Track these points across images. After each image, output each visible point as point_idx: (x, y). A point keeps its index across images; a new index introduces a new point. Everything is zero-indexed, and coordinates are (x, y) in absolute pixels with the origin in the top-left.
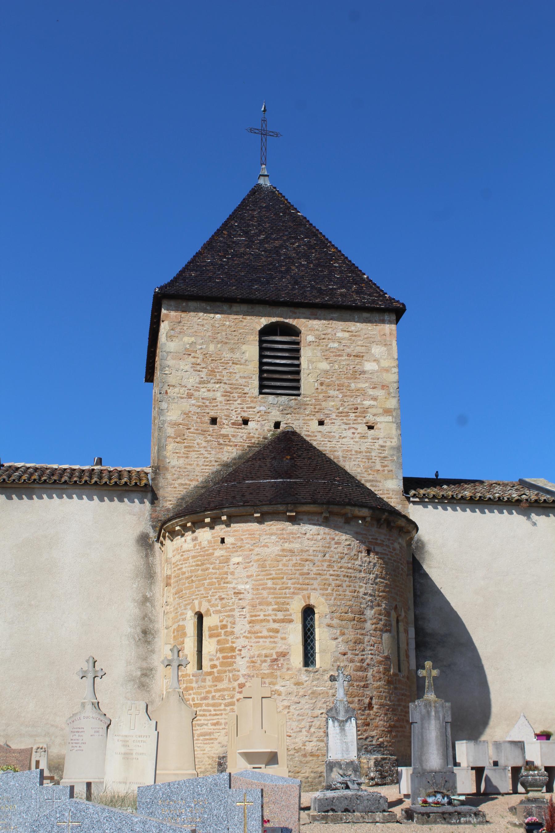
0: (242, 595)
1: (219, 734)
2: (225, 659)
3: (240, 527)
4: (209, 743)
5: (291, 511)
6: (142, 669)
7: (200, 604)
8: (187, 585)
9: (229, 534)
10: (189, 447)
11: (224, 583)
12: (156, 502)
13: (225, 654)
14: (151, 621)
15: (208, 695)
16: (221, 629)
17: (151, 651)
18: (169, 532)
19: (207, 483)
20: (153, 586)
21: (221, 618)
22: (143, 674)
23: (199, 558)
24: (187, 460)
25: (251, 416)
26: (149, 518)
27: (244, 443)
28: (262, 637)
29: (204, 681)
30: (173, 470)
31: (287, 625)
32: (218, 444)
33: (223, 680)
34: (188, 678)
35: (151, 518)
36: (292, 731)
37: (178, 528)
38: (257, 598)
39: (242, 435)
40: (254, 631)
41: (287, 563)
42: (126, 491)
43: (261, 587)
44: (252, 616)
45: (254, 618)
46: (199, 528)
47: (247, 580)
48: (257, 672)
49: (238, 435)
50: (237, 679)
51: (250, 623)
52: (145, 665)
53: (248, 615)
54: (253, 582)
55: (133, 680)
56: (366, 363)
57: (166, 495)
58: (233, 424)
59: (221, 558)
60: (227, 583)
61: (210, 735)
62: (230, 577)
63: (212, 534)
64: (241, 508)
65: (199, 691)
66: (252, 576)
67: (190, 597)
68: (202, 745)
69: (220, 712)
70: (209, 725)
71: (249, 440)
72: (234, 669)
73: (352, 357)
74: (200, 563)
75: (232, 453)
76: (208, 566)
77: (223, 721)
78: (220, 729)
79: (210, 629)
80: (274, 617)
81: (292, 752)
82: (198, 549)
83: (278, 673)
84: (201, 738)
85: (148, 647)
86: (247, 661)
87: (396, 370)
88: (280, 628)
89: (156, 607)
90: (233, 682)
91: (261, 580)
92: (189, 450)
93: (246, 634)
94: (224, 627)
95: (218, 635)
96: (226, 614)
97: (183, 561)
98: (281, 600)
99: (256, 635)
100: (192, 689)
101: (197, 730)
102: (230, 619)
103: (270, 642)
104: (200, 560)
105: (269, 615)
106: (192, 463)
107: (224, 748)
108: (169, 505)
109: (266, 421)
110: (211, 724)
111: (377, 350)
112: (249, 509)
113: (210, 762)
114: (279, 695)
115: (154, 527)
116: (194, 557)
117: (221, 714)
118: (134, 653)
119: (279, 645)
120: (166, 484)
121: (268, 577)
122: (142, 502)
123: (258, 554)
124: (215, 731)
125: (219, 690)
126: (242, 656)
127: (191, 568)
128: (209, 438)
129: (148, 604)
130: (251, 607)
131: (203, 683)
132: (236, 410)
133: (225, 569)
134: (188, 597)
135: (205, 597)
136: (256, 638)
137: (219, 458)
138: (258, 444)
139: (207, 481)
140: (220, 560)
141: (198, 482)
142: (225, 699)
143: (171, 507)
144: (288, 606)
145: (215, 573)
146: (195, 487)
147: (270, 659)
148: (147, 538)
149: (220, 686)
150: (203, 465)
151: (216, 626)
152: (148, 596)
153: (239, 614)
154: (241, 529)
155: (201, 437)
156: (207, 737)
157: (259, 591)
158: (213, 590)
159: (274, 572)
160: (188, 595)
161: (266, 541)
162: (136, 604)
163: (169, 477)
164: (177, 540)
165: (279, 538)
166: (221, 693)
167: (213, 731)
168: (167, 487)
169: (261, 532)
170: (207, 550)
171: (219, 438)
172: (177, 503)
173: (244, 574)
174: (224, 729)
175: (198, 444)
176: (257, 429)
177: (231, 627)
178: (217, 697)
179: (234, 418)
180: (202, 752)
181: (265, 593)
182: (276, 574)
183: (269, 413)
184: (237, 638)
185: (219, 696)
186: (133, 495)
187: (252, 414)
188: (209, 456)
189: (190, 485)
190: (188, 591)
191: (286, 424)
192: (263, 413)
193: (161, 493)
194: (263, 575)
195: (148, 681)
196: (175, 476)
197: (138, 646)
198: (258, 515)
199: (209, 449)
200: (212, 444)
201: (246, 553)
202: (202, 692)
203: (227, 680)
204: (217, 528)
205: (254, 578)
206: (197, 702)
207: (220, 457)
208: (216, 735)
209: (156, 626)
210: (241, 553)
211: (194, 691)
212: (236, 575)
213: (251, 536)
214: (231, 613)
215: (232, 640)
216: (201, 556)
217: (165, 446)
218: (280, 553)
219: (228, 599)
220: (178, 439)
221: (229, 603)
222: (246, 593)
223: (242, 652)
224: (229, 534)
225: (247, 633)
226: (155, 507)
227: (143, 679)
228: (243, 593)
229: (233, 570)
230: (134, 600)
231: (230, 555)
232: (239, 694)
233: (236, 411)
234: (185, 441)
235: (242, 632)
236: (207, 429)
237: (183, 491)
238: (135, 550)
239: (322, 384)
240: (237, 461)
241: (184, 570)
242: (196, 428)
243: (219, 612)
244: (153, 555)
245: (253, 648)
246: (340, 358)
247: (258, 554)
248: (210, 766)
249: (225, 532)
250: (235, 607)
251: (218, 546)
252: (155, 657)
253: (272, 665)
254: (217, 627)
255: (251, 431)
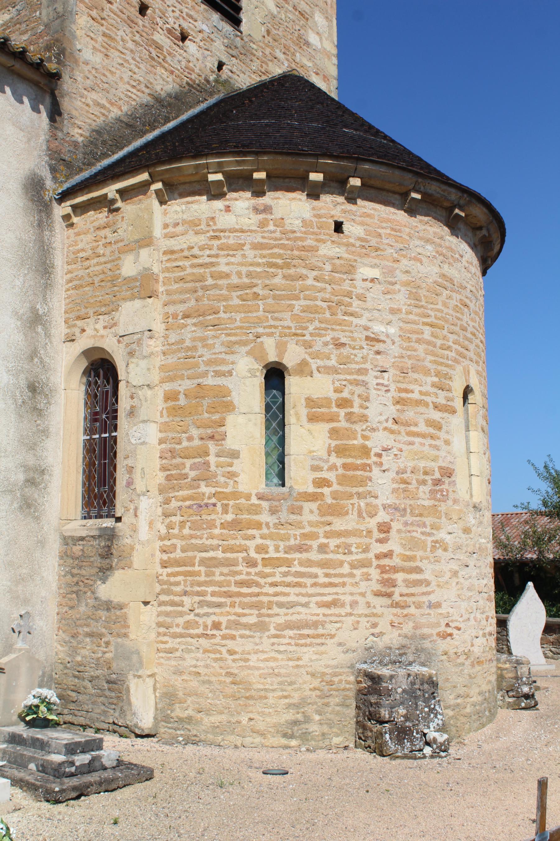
0: (381, 344)
1: (338, 625)
2: (349, 470)
3: (373, 209)
4: (311, 645)
5: (461, 209)
6: (27, 468)
7: (281, 348)
8: (236, 302)
9: (353, 217)
10: (110, 37)
11: (345, 314)
12: (58, 118)
13: (350, 460)
14: (44, 367)
15: (309, 543)
16: (338, 406)
17: (43, 431)
18: (164, 184)
19: (133, 119)
20: (48, 292)
21: (337, 384)
22: (27, 481)
23: (276, 250)
24: (106, 60)
25: (191, 33)
26: (44, 147)
27: (182, 73)
28: (418, 435)
29: (298, 511)
30: (86, 68)
31: (449, 416)
32: (150, 57)
33: (347, 513)
34: (243, 501)
35: (49, 149)
36: (461, 619)
37: (212, 177)
38: (409, 357)
39: (181, 58)
40: (404, 421)
41: (447, 301)
42: (11, 71)
43: (414, 337)
44: (400, 390)
45: (404, 395)
46: (276, 189)
47: (390, 317)
48: (412, 502)
49: (175, 56)
50: (373, 513)
51: (398, 402)
52: (31, 461)
53: (393, 387)
54: (401, 324)
55: (11, 491)
56: (310, 31)
57: (74, 113)
58: (169, 31)
59: (337, 262)
60: (352, 315)
61: (316, 628)
62: (356, 303)
63: (313, 209)
64: (397, 172)
65: (282, 532)
66: (399, 310)
67: (248, 328)
68: (290, 648)
69: (341, 580)
70: (311, 605)
71: (188, 73)
72: (370, 492)
73: (297, 13)
74: (279, 261)
75: (167, 82)
76: (304, 271)
77: (348, 599)
78: (340, 615)
79: (310, 402)
80: (435, 400)
81: (461, 659)
82: (274, 232)
83: (443, 507)
84: (291, 633)
85: (38, 422)
86: (393, 480)
87: (335, 61)
88: (443, 422)
89: (53, 340)
90: (368, 519)
91: (414, 322)
92: (109, 42)
93: (390, 424)
94: (344, 403)
95: (332, 419)
96: (348, 377)
97: (220, 248)
98: (443, 368)
99: (408, 429)
100: (258, 525)
101: (278, 615)
102: (359, 390)
103: (430, 445)
104: (280, 256)
105: (427, 394)
106: (113, 70)
107: (350, 655)
108: (77, 136)
109: (209, 53)
110: (317, 603)
111: (319, 19)
112: (408, 179)
113: (316, 683)
114: (445, 550)
115: (53, 170)
116: (256, 246)
117: (344, 584)
118: (12, 430)
119: (442, 454)
120: (74, 91)
121: (425, 320)
122: (36, 109)
123: (407, 272)
124: (327, 619)
125: (339, 534)
126: (383, 468)
127: (251, 269)
128: (137, 38)
129: (40, 329)
130: (398, 373)
131: (293, 517)
132: (174, 9)
133: (346, 286)
134: (241, 328)
135: (295, 334)
136: (409, 434)
137: (151, 83)
138: (199, 85)
139: (133, 116)
140: (334, 265)
141: (122, 111)
142: (350, 553)
143: (80, 139)
144: (451, 383)
145: (323, 290)
146: (116, 119)
147: (432, 479)
148: (41, 188)
149: (339, 524)
150: (128, 83)
151: (326, 398)
152: (40, 312)
153: (376, 381)
154: (376, 213)
155: (128, 30)
156: (306, 632)
157: (412, 344)
158: (317, 324)
159: (432, 313)
160: (238, 324)
161: (419, 250)
162: (19, 323)
163: (79, 79)
164: (188, 203)
165: (437, 252)
166: (343, 539)
167: (324, 619)
168: (75, 98)
169: (412, 232)
170: (302, 239)
171: (151, 46)
172: (91, 137)
173: (385, 304)
174: (351, 614)
175: (123, 40)
176: (198, 60)
177: (361, 406)
178: (332, 548)
179: (171, 20)
180: (291, 663)
181: (421, 349)
182: (435, 316)
183: (212, 40)
184: (373, 430)
185: (338, 547)
186: (22, 86)
187: (193, 30)
188: (136, 70)
189: (109, 111)
190: (239, 316)
191: (232, 72)
192: (206, 35)
193: (66, 104)
194: (416, 315)
195: (36, 496)
196: (88, 82)
197: (21, 416)
198: (418, 196)
199: (138, 59)
200: (141, 50)
201: (387, 263)
202: (289, 535)
203: (355, 513)
204: (327, 199)
205: (403, 316)
206: (272, 554)
207: (151, 80)
208: (331, 628)
209: (52, 378)
210: (376, 261)
211: (265, 531)
212: (369, 304)
213: (395, 233)
214: (360, 378)
215: (364, 433)
216: (283, 247)
217: (74, 13)
218: (440, 280)
219: (354, 348)
220: (94, 13)
221: (356, 355)
222: (388, 341)
223: (384, 459)
224: (353, 217)
225: (391, 421)
226: (56, 128)
227: (28, 491)
228: (384, 342)
229: (360, 291)
230: (17, 313)
231: (355, 261)
232: (378, 544)
233: (173, 11)
234: (103, 22)
235: (383, 418)
236: (136, 20)
237: (99, 118)
238: (21, 205)
239: (268, 32)
240: (172, 101)
241: (224, 268)
242: (120, 7)
243: (334, 371)
244: (51, 227)
245: (404, 454)
246: (286, 5)
247: (407, 272)
248: (318, 693)
249: (344, 211)
250: (368, 366)
251: (328, 234)
252: (49, 444)
253: (435, 490)
254: (327, 402)
255: (191, 59)
